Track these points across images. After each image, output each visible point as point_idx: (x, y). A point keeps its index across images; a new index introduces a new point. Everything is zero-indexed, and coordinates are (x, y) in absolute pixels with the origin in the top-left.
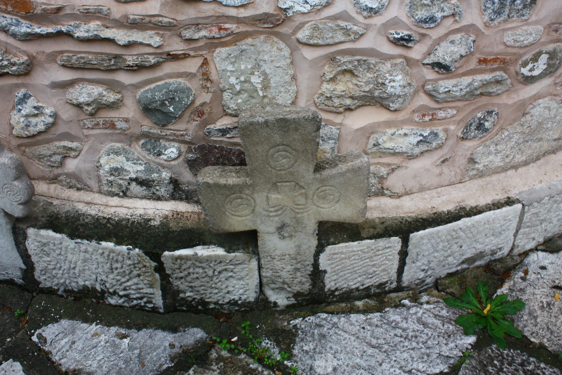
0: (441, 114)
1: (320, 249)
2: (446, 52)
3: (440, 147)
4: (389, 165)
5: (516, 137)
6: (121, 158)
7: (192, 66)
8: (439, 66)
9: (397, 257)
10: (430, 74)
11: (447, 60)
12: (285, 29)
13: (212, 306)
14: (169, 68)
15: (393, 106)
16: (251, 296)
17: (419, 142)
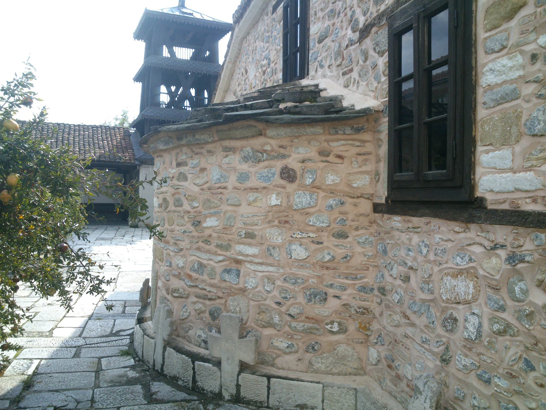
2: (294, 311)
3: (297, 352)
4: (277, 354)
5: (331, 359)
6: (202, 332)
7: (223, 301)
8: (290, 315)
9: (266, 388)
10: (289, 318)
11: (293, 314)
12: (246, 293)
13: (205, 392)
14: (218, 301)
15: (278, 328)
16: (217, 390)
17: (288, 347)
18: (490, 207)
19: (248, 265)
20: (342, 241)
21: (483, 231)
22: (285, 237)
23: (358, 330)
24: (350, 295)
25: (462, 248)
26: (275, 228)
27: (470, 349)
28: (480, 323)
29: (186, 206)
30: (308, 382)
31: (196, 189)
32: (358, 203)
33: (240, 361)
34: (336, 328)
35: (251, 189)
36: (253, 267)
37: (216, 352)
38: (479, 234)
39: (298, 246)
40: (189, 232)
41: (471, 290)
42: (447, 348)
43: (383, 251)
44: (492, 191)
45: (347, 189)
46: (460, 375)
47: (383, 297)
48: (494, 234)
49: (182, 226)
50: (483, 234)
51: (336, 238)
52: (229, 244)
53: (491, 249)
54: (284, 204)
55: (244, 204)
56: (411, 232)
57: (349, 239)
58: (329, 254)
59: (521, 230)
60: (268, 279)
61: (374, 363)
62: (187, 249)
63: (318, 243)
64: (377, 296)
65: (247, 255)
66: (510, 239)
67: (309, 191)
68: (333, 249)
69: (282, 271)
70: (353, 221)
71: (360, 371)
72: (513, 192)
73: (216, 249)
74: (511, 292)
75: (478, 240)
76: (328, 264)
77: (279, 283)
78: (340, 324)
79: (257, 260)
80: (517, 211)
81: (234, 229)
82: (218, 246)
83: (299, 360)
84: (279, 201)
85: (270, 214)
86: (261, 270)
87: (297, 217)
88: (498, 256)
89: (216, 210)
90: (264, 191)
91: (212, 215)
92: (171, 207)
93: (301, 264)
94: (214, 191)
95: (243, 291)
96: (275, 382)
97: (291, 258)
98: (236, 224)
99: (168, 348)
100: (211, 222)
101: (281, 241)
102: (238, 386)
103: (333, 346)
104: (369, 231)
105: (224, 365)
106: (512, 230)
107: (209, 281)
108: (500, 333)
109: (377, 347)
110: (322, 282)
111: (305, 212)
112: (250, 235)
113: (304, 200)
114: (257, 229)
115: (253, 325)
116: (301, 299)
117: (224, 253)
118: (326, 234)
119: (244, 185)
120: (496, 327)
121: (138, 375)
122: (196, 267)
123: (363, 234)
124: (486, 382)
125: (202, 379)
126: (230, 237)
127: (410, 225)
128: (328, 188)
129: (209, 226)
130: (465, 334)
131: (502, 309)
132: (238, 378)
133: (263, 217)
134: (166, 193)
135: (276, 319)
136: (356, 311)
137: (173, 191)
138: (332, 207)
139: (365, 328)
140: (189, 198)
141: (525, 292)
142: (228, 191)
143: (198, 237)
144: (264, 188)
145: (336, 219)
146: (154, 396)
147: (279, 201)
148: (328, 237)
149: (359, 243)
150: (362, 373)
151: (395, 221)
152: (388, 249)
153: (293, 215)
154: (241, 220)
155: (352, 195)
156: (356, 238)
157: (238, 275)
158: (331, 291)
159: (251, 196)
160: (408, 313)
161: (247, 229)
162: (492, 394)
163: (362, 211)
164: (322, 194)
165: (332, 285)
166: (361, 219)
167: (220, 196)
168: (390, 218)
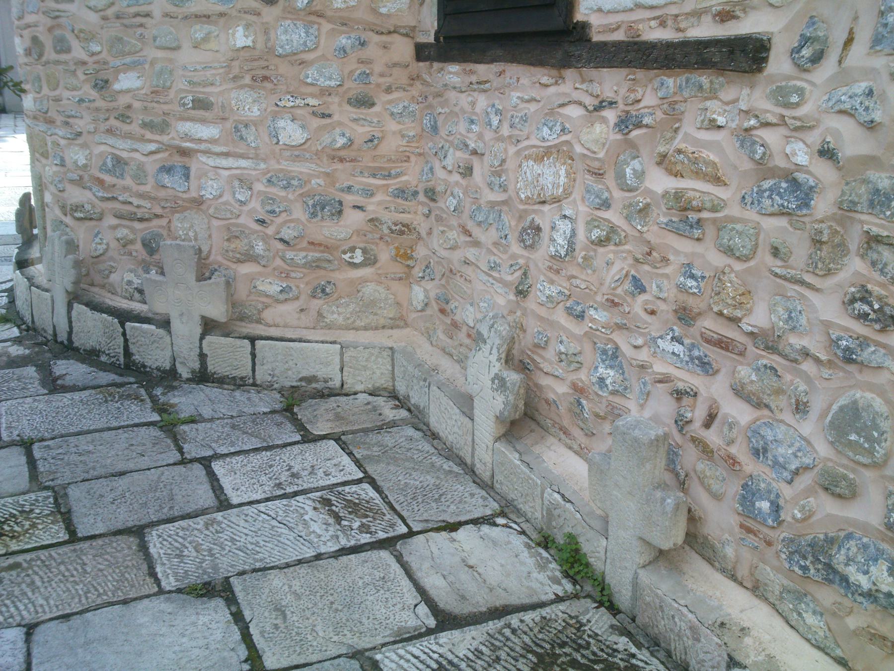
0: (293, 275)
1: (202, 338)
2: (288, 233)
3: (297, 298)
4: (263, 303)
5: (352, 306)
6: (132, 275)
7: (163, 222)
8: (281, 240)
9: (250, 357)
10: (280, 246)
11: (286, 238)
12: (204, 207)
13: (148, 369)
14: (155, 222)
15: (263, 263)
16: (167, 365)
17: (281, 291)
18: (596, 38)
19: (203, 158)
20: (364, 111)
21: (583, 81)
22: (264, 106)
23: (394, 259)
24: (379, 203)
25: (552, 112)
26: (247, 89)
27: (558, 272)
28: (573, 231)
29: (78, 52)
30: (317, 342)
31: (93, 18)
32: (390, 43)
33: (203, 317)
34: (358, 257)
35: (196, 16)
36: (211, 161)
37: (159, 305)
38: (577, 85)
39: (289, 121)
40: (90, 101)
41: (563, 180)
42: (525, 274)
43: (432, 127)
44: (600, 10)
45: (371, 18)
46: (542, 311)
47: (432, 204)
48: (600, 84)
49: (74, 89)
50: (584, 86)
51: (355, 106)
52: (164, 121)
53: (595, 110)
54: (260, 45)
55: (186, 45)
56: (475, 91)
57: (376, 109)
58: (344, 135)
59: (640, 74)
60: (241, 180)
61: (419, 308)
62: (89, 132)
63: (324, 116)
64: (422, 204)
65: (200, 141)
66: (623, 91)
67: (303, 20)
68: (351, 127)
69: (263, 166)
70: (382, 75)
71: (399, 322)
72: (631, 10)
73: (143, 131)
74: (620, 176)
75: (576, 95)
76: (342, 153)
77: (259, 187)
78: (365, 251)
79: (218, 149)
80: (636, 43)
81: (172, 94)
82: (145, 125)
83: (302, 310)
84: (250, 39)
85: (236, 63)
86: (226, 166)
87: (284, 68)
88: (604, 120)
89: (135, 58)
90: (222, 21)
91: (128, 68)
92: (50, 54)
93: (296, 153)
94: (126, 22)
95: (198, 203)
96: (264, 346)
97: (277, 143)
98: (175, 84)
99: (75, 305)
100: (127, 82)
101: (259, 113)
102: (202, 356)
103: (356, 286)
104: (409, 93)
105: (175, 324)
106: (627, 75)
107: (135, 188)
108: (601, 242)
109: (423, 283)
110: (333, 184)
111: (297, 59)
112: (202, 104)
113: (295, 37)
114: (213, 93)
115: (220, 258)
116: (299, 213)
117: (157, 137)
118: (336, 100)
119: (184, 10)
120: (596, 234)
121: (27, 352)
122: (110, 164)
123: (400, 99)
124: (578, 316)
125: (141, 349)
126: (165, 107)
127: (474, 79)
128: (337, 14)
129: (124, 88)
130: (552, 249)
131: (606, 205)
132: (201, 344)
133: (221, 71)
134: (36, 26)
135: (260, 248)
136: (391, 229)
137: (49, 22)
138: (345, 51)
139: (405, 256)
140: (82, 35)
141: (640, 175)
142: (154, 22)
143: (108, 110)
144: (222, 15)
145: (351, 72)
146: (59, 382)
147: (250, 39)
148: (340, 105)
149: (392, 114)
150: (402, 324)
151: (450, 73)
152: (439, 124)
153: (276, 66)
154: (184, 76)
155: (378, 28)
156: (388, 106)
157: (187, 177)
158: (349, 199)
159: (199, 31)
160: (470, 225)
161: (196, 92)
162: (586, 333)
163: (396, 58)
164: (326, 27)
165: (349, 188)
166: (396, 71)
167: (140, 31)
168: (442, 69)
